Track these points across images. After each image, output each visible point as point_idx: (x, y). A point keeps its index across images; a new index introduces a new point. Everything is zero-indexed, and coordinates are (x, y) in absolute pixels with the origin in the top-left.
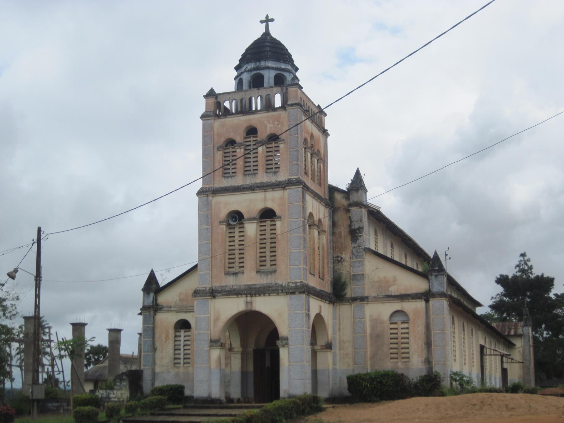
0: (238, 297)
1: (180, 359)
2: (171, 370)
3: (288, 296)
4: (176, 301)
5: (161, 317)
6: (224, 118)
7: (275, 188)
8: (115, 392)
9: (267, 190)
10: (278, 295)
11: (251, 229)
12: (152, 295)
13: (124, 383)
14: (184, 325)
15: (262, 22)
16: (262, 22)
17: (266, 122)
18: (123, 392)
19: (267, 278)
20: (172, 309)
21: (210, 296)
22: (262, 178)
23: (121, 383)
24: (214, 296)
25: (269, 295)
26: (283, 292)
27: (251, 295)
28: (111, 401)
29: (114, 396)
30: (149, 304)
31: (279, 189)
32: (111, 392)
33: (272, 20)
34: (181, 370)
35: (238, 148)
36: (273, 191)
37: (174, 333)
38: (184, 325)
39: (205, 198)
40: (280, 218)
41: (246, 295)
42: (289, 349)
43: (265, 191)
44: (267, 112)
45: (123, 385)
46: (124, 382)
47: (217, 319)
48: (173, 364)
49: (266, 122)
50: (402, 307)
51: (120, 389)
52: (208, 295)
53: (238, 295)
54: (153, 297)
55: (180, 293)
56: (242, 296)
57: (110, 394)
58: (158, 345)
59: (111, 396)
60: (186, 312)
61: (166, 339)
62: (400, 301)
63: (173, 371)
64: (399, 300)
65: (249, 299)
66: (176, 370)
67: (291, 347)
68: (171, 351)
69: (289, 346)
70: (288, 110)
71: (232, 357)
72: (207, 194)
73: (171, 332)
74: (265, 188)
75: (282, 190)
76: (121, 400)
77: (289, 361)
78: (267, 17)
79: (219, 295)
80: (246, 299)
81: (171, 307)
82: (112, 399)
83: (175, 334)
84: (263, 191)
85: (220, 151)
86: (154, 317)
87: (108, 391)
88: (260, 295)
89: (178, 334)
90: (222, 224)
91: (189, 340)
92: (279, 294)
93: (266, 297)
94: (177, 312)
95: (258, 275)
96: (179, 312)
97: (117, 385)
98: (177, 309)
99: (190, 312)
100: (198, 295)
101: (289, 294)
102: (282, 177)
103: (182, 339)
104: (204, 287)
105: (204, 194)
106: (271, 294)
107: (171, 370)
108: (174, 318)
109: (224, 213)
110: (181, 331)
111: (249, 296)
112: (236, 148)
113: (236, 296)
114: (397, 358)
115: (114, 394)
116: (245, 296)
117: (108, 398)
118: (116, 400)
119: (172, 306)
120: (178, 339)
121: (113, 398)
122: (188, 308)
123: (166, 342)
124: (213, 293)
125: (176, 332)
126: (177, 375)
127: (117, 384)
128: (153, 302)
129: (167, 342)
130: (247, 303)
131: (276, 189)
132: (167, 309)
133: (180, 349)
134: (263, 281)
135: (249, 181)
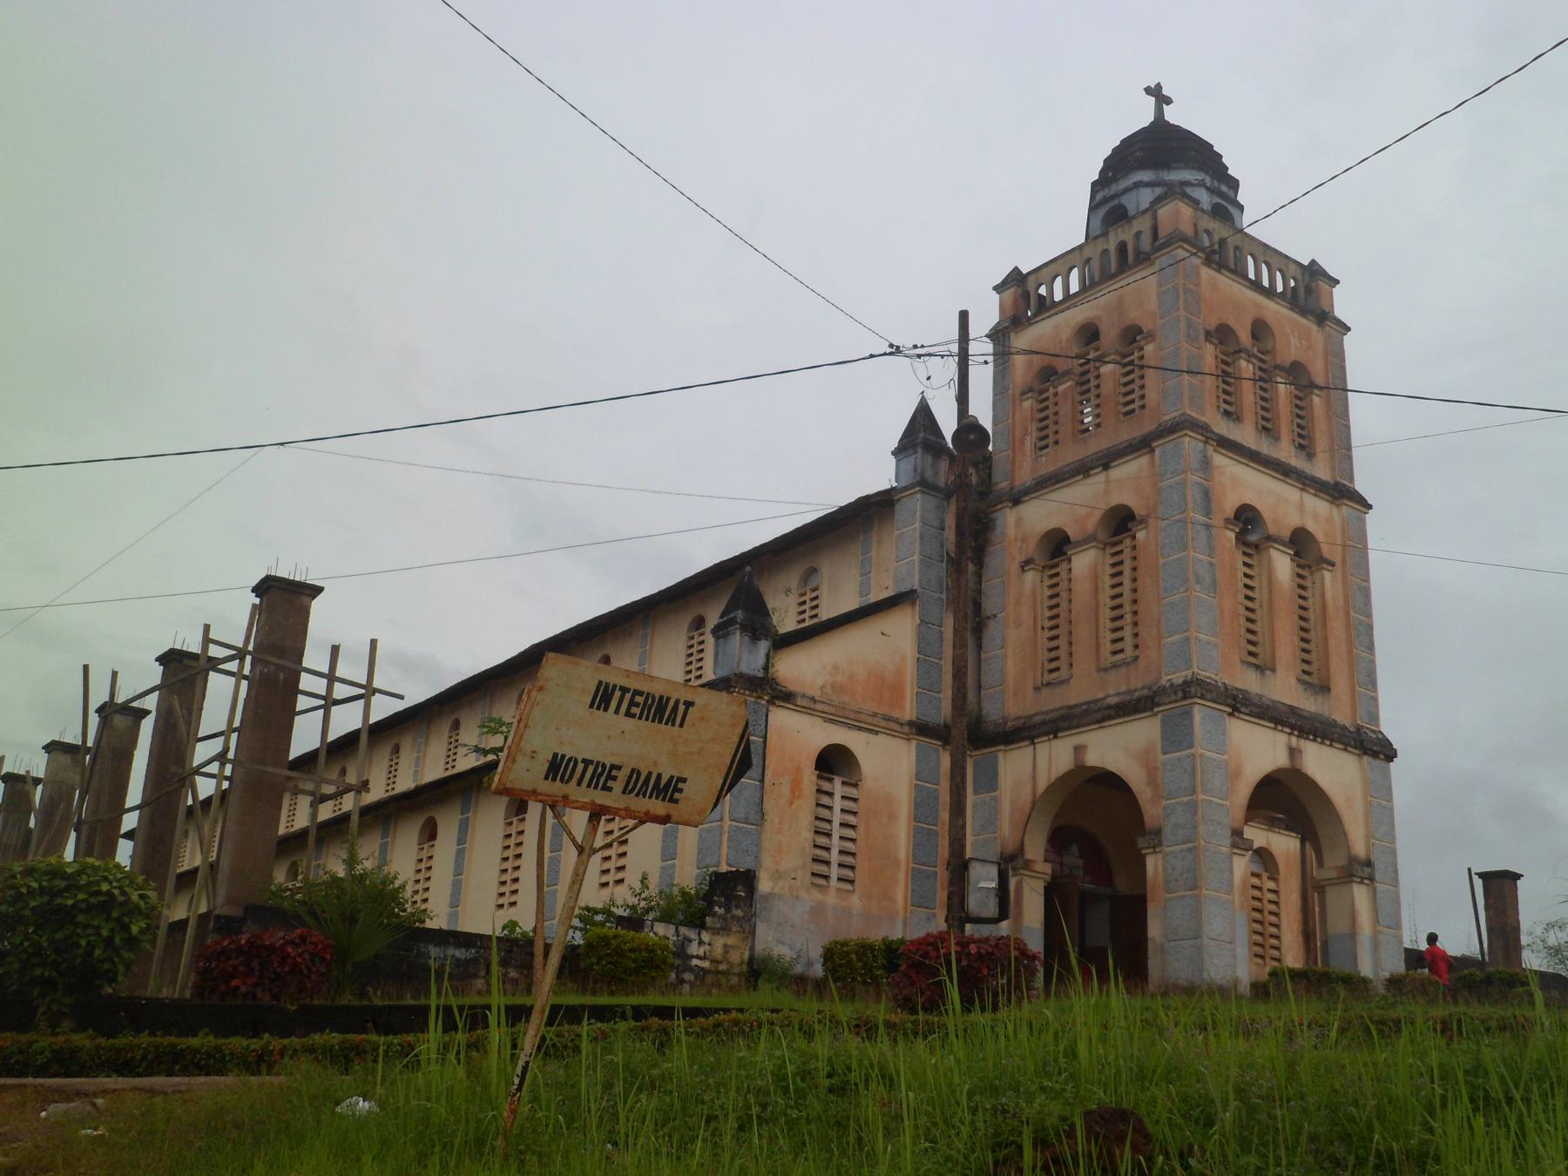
0: (1275, 729)
1: (827, 863)
2: (803, 894)
3: (1366, 758)
4: (823, 687)
5: (782, 719)
6: (1215, 270)
7: (1320, 491)
8: (706, 937)
9: (1307, 488)
10: (1345, 750)
11: (1282, 564)
12: (763, 646)
13: (739, 913)
14: (833, 762)
15: (1148, 91)
16: (1148, 91)
17: (1288, 331)
18: (731, 941)
19: (1315, 700)
20: (819, 707)
21: (1229, 706)
22: (1285, 452)
23: (728, 910)
24: (1235, 711)
25: (1331, 745)
26: (1355, 748)
27: (1299, 731)
28: (691, 969)
29: (701, 952)
30: (752, 673)
31: (1327, 497)
32: (692, 934)
33: (1168, 101)
34: (831, 899)
35: (1244, 359)
36: (1315, 495)
37: (815, 778)
38: (833, 762)
39: (1201, 445)
40: (1332, 564)
41: (1292, 727)
42: (1374, 891)
43: (1302, 489)
44: (1292, 309)
45: (733, 917)
46: (737, 907)
47: (1237, 774)
48: (808, 878)
49: (1288, 331)
50: (1268, 842)
51: (725, 930)
52: (1229, 701)
53: (1276, 724)
54: (768, 656)
55: (836, 667)
56: (1285, 729)
57: (690, 941)
58: (769, 805)
59: (694, 949)
60: (851, 727)
61: (792, 792)
62: (1266, 827)
63: (810, 897)
64: (1264, 824)
65: (1294, 740)
66: (817, 895)
67: (1380, 887)
68: (807, 835)
69: (1376, 884)
70: (1327, 328)
71: (1024, 884)
72: (1207, 438)
73: (809, 776)
74: (1307, 482)
75: (1328, 501)
76: (723, 967)
77: (1376, 921)
78: (1159, 86)
79: (1243, 709)
80: (1289, 739)
81: (813, 699)
82: (695, 962)
83: (817, 785)
84: (1300, 486)
85: (1211, 342)
86: (767, 716)
87: (684, 930)
88: (1314, 740)
89: (826, 786)
90: (1232, 527)
91: (855, 813)
92: (1349, 749)
93: (1323, 747)
94: (826, 720)
95: (1301, 688)
96: (832, 721)
97: (714, 914)
98: (833, 712)
99: (860, 729)
100: (1209, 696)
101: (1368, 755)
102: (1321, 470)
103: (838, 804)
104: (1210, 678)
105: (1202, 435)
106: (1334, 744)
107: (803, 894)
108: (818, 735)
109: (1230, 504)
110: (830, 780)
111: (1296, 733)
112: (1243, 355)
113: (1272, 725)
114: (1262, 957)
115: (701, 943)
116: (1289, 731)
117: (682, 953)
118: (706, 964)
119: (817, 698)
120: (825, 800)
121: (698, 957)
122: (862, 717)
123: (791, 803)
124: (1238, 703)
125: (819, 777)
126: (817, 911)
127: (717, 909)
128: (766, 668)
129: (797, 803)
130: (1293, 752)
131: (1322, 495)
132: (805, 703)
133: (828, 835)
134: (1309, 704)
135: (1264, 447)
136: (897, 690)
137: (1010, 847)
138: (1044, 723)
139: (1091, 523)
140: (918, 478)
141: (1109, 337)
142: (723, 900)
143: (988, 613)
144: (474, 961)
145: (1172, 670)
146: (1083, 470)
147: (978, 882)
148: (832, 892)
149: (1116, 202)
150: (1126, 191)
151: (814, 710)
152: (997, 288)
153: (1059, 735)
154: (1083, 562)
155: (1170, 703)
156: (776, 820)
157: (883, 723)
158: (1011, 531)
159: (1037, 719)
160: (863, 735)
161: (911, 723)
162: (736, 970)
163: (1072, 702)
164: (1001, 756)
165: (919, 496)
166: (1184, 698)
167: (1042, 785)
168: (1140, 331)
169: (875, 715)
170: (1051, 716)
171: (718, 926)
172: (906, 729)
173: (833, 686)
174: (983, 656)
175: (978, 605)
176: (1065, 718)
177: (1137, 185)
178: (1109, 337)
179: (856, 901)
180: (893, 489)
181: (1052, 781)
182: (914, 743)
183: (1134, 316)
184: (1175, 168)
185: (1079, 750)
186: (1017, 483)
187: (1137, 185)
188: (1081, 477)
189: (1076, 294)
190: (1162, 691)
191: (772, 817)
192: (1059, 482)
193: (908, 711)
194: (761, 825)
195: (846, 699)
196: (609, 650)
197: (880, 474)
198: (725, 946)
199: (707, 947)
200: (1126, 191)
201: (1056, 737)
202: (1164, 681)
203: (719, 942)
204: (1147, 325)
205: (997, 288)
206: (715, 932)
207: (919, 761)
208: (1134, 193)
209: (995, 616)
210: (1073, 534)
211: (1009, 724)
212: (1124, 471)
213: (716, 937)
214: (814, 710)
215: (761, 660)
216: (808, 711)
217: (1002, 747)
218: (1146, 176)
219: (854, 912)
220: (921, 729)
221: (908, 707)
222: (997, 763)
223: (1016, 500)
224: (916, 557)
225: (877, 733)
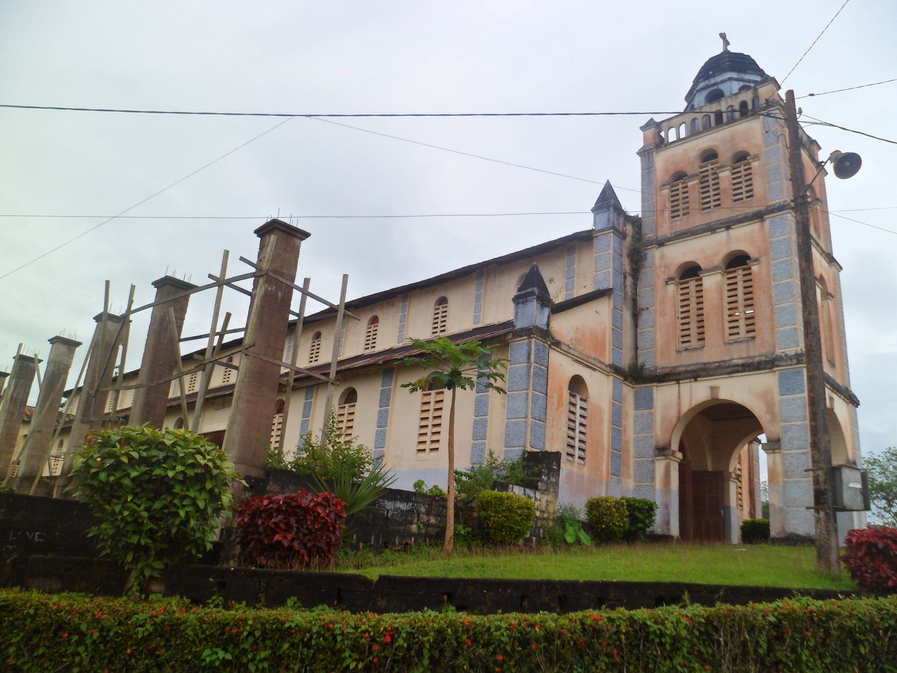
4: (571, 340)
12: (547, 311)
18: (550, 498)
20: (572, 351)
45: (551, 482)
54: (549, 317)
61: (558, 403)
73: (566, 392)
76: (545, 515)
96: (576, 361)
97: (542, 481)
98: (577, 355)
99: (588, 367)
122: (590, 360)
123: (558, 409)
127: (543, 477)
129: (560, 409)
136: (602, 345)
137: (661, 443)
138: (687, 372)
139: (718, 260)
140: (611, 225)
141: (725, 156)
142: (546, 471)
143: (643, 306)
144: (411, 512)
145: (784, 347)
146: (711, 229)
147: (849, 483)
148: (576, 465)
149: (715, 87)
150: (723, 81)
151: (569, 353)
152: (642, 128)
153: (699, 379)
154: (712, 282)
155: (787, 365)
156: (551, 419)
157: (599, 365)
158: (657, 261)
159: (681, 369)
160: (589, 371)
161: (610, 366)
162: (551, 517)
163: (705, 361)
164: (655, 388)
165: (612, 235)
166: (797, 364)
167: (685, 408)
168: (749, 155)
169: (595, 359)
170: (692, 368)
171: (544, 488)
172: (608, 369)
173: (576, 338)
174: (639, 331)
175: (635, 301)
176: (704, 370)
177: (730, 79)
178: (725, 156)
179: (586, 470)
180: (593, 230)
181: (693, 405)
182: (611, 378)
183: (742, 146)
184: (749, 74)
185: (713, 389)
186: (659, 235)
187: (730, 79)
188: (709, 233)
189: (684, 139)
190: (779, 359)
191: (549, 417)
192: (692, 235)
193: (608, 359)
194: (544, 421)
195: (581, 348)
196: (377, 313)
197: (586, 223)
198: (547, 501)
199: (539, 502)
200: (723, 81)
201: (696, 380)
202: (778, 352)
203: (545, 498)
204: (753, 151)
205: (642, 128)
206: (544, 492)
207: (614, 389)
208: (728, 83)
209: (647, 309)
210: (702, 267)
211: (658, 371)
212: (739, 232)
213: (543, 496)
214: (569, 353)
215: (545, 320)
216: (566, 353)
217: (656, 384)
218: (734, 75)
219: (585, 477)
220: (616, 370)
221: (607, 356)
222: (652, 393)
223: (661, 244)
224: (611, 270)
225: (595, 370)
